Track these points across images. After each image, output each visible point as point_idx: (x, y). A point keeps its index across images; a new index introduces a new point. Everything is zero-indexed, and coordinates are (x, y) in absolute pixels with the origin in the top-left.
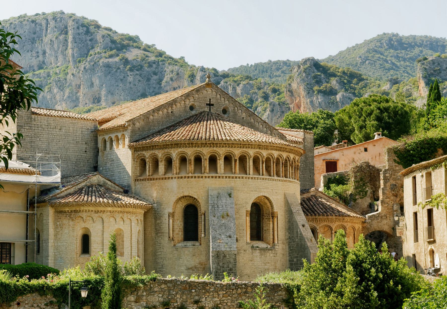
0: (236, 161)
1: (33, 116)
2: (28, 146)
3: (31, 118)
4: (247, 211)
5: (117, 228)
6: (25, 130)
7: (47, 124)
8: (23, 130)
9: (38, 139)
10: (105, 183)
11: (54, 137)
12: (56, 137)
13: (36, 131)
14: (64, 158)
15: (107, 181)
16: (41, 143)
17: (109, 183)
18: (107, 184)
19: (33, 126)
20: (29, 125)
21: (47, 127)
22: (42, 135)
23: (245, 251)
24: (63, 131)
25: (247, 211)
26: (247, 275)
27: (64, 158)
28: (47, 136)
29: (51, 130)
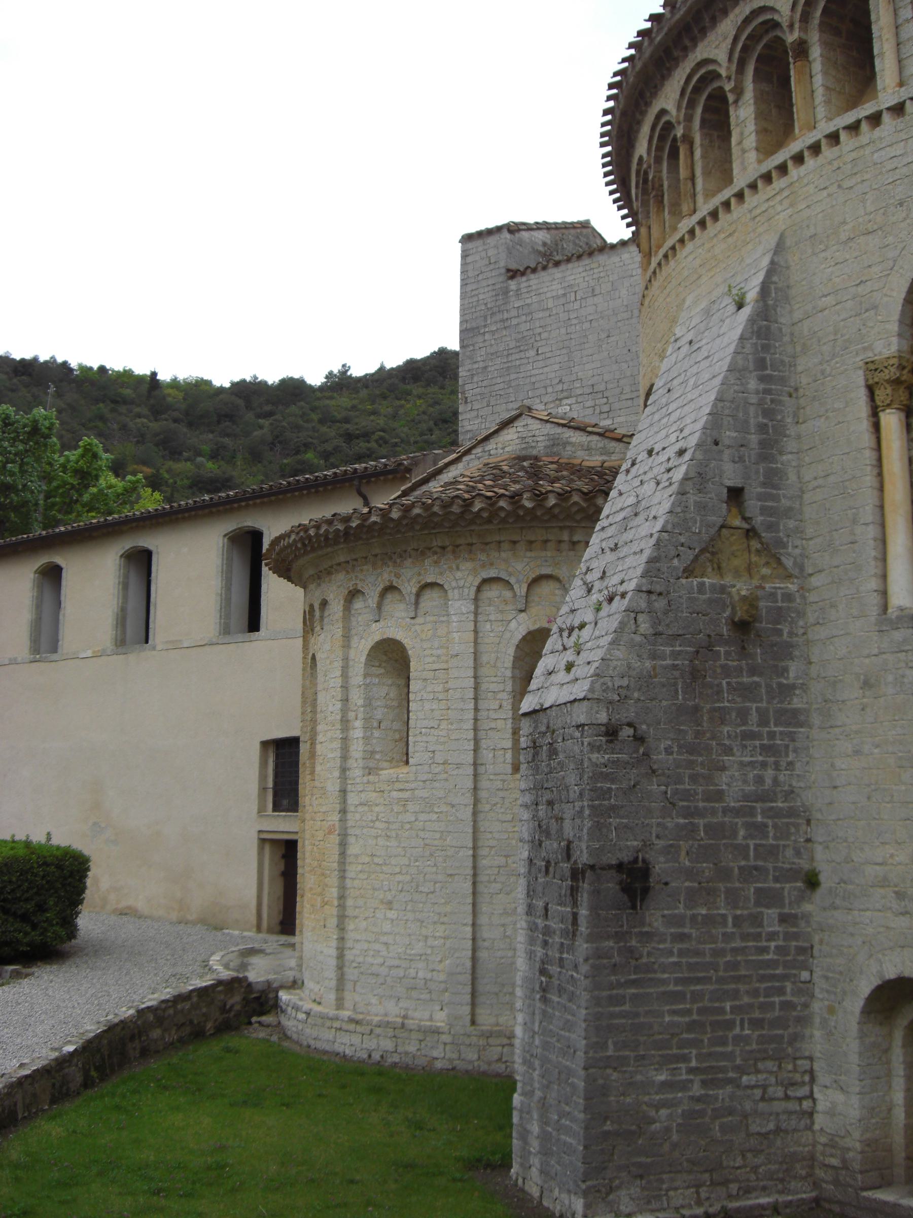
0: (802, 49)
1: (513, 285)
2: (497, 387)
3: (506, 292)
4: (871, 367)
5: (377, 638)
6: (487, 337)
7: (561, 292)
8: (480, 339)
9: (532, 353)
10: (555, 443)
11: (586, 325)
12: (594, 324)
13: (523, 327)
14: (627, 389)
15: (568, 434)
16: (541, 364)
17: (577, 437)
18: (566, 444)
19: (514, 313)
20: (499, 317)
21: (562, 300)
22: (544, 335)
23: (867, 684)
24: (624, 292)
25: (871, 367)
26: (884, 882)
27: (627, 389)
28: (563, 331)
29: (576, 305)
